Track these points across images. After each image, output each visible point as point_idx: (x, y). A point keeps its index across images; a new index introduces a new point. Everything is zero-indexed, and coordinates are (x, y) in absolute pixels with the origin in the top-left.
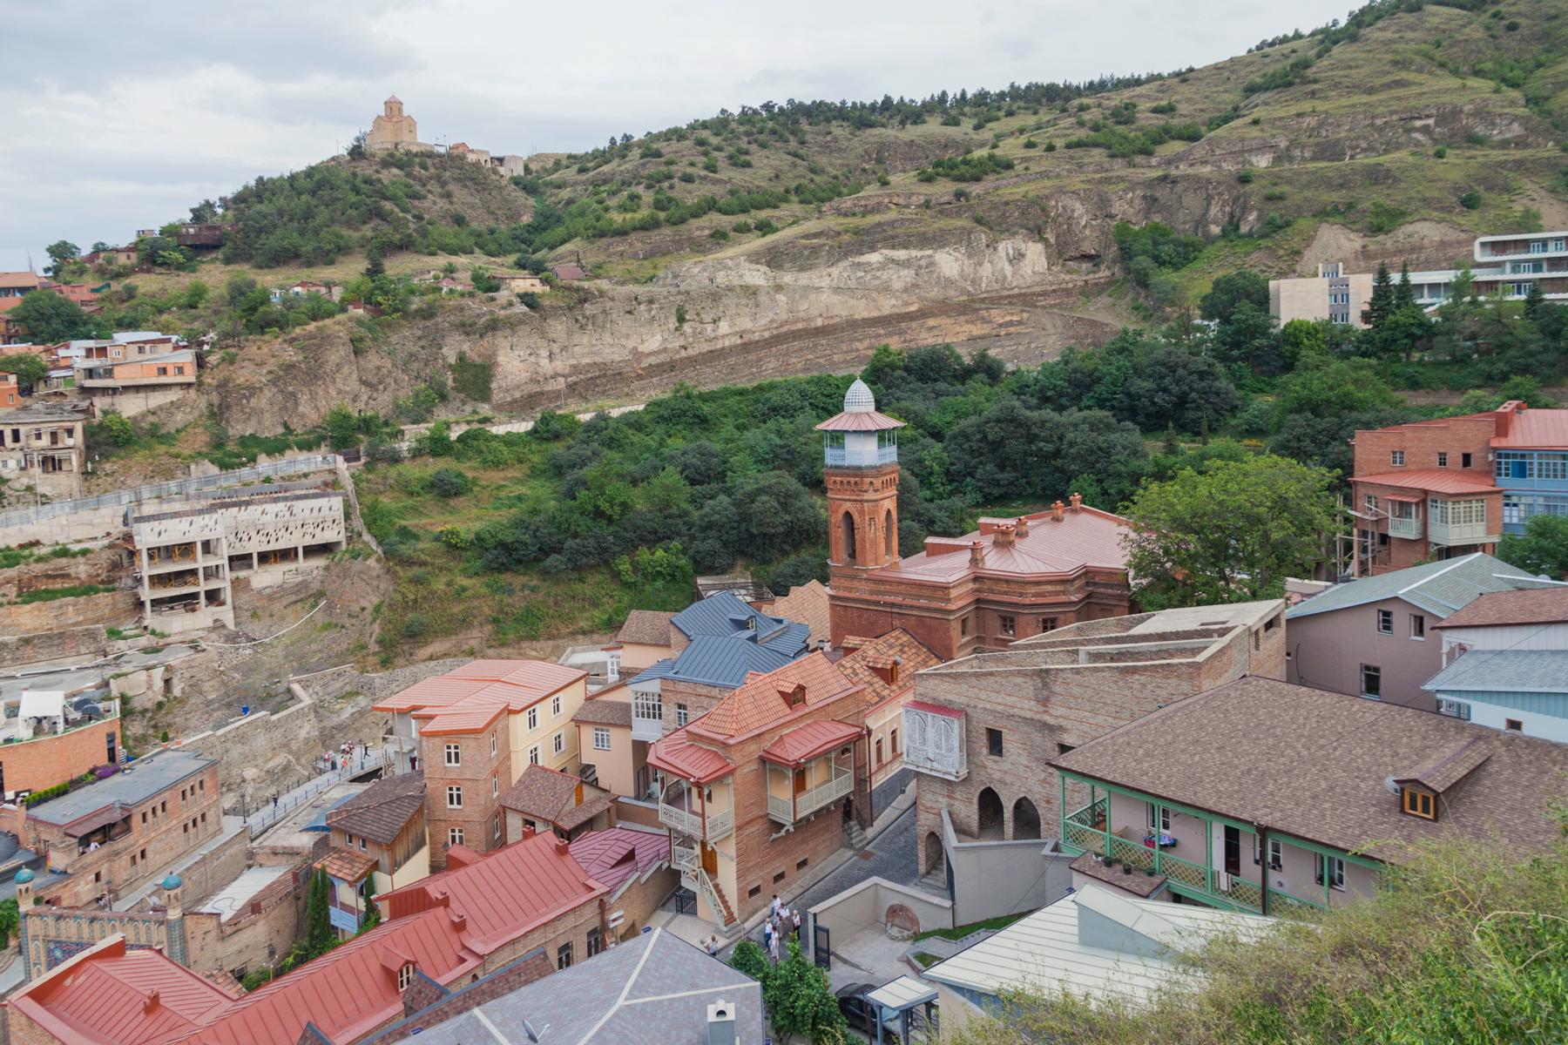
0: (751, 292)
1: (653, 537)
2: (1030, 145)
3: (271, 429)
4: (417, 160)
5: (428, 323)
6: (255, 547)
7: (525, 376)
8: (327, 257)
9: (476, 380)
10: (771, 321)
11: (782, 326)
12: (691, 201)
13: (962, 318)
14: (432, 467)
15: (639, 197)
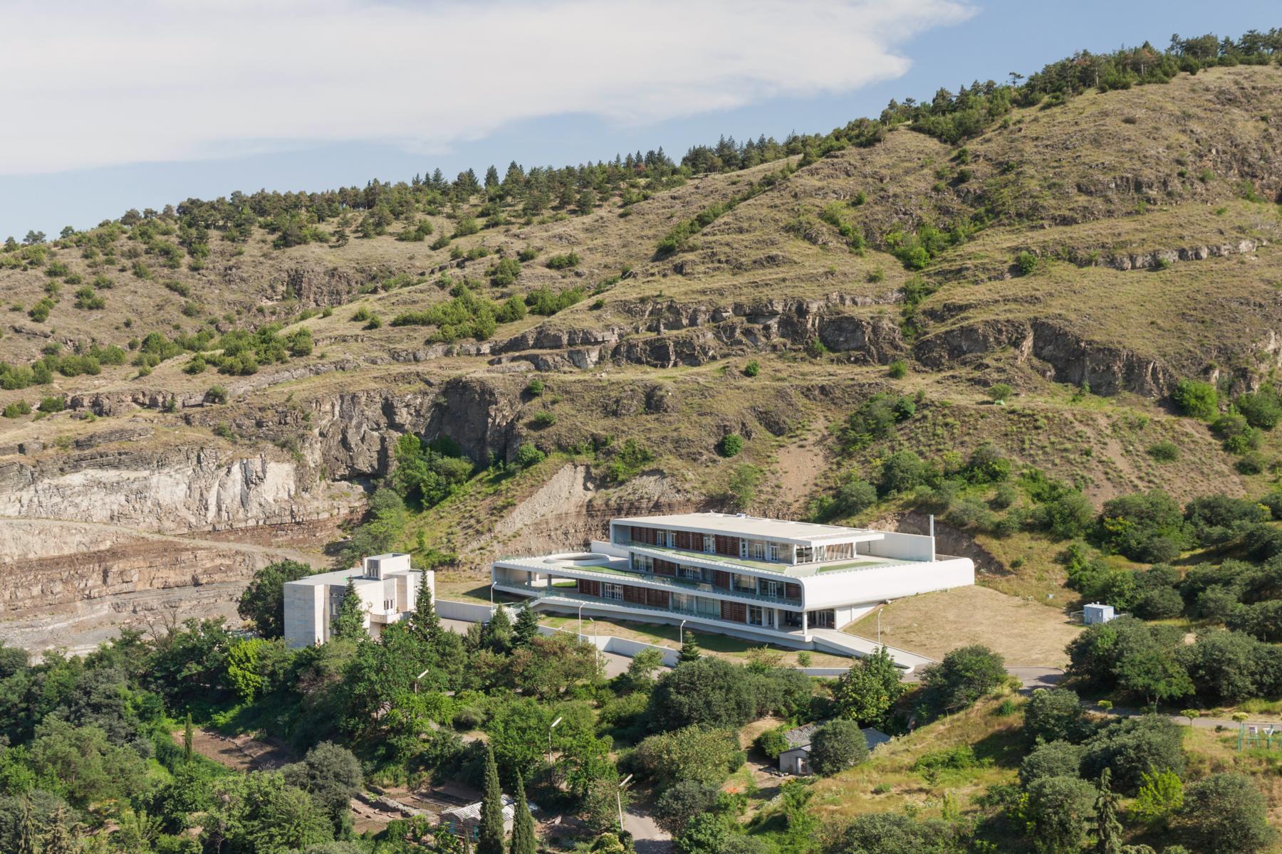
13: (159, 561)
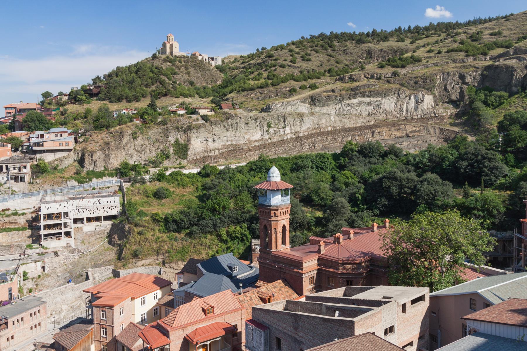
0: (301, 116)
1: (235, 221)
2: (430, 51)
3: (100, 168)
4: (178, 59)
5: (164, 127)
6: (85, 215)
7: (202, 149)
8: (137, 99)
9: (182, 150)
10: (308, 128)
11: (313, 130)
12: (283, 75)
13: (393, 129)
14: (158, 185)
15: (262, 74)
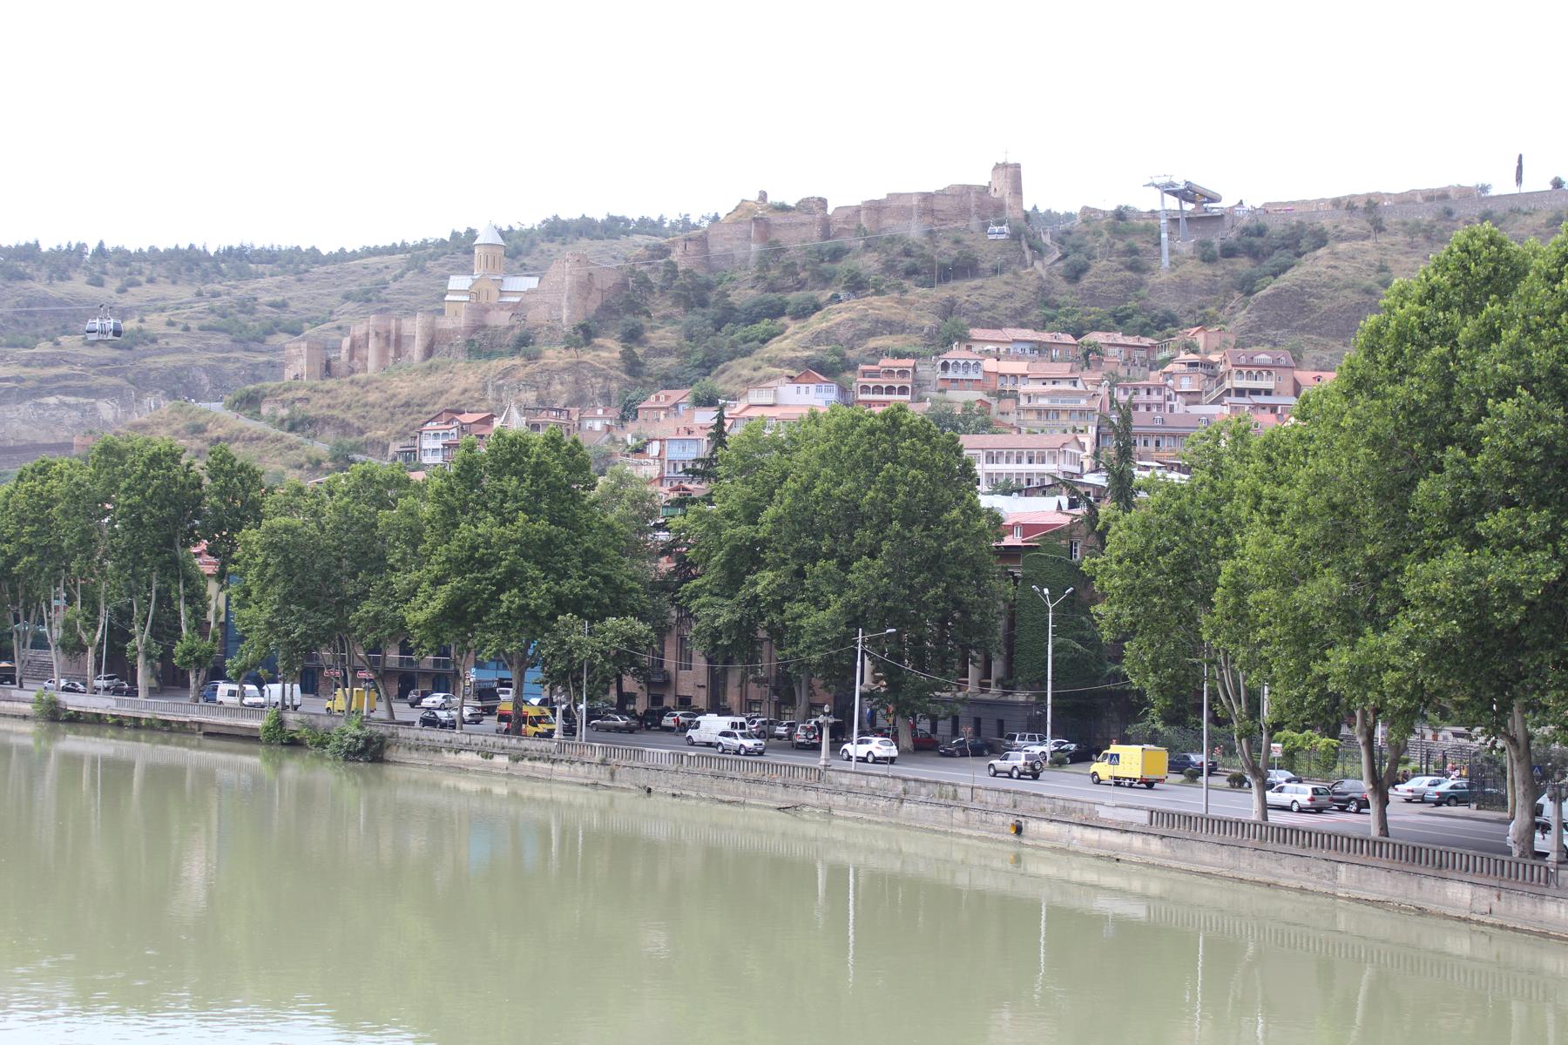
2: (171, 324)
